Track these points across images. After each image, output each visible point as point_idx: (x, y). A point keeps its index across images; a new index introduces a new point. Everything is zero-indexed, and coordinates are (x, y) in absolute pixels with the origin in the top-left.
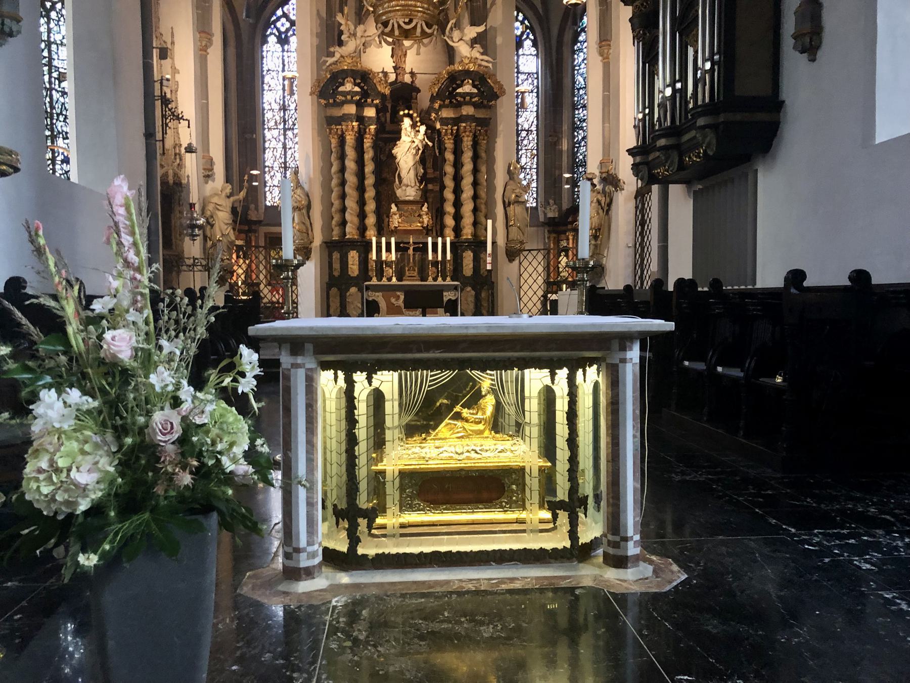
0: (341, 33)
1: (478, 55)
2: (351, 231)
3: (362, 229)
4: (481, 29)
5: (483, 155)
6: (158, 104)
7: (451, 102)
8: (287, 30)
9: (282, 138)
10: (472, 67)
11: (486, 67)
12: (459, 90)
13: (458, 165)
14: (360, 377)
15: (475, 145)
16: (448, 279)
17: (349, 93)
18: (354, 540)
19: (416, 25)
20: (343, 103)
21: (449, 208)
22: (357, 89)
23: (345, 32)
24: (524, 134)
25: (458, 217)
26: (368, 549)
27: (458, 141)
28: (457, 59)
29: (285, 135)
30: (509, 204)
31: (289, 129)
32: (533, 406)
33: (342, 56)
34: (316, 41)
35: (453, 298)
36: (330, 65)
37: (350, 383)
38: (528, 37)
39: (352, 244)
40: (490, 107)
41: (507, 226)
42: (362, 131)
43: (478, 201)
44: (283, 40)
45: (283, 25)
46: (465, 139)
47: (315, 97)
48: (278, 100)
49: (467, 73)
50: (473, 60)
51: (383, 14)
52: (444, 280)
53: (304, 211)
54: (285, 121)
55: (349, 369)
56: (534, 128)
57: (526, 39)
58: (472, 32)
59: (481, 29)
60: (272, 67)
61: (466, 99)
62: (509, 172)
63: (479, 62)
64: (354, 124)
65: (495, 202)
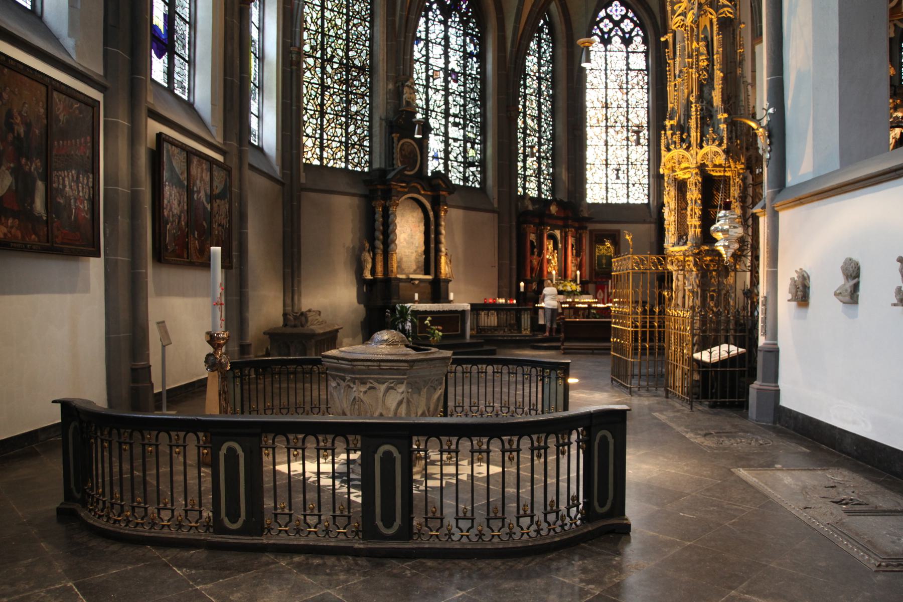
8: (611, 30)
9: (604, 135)
29: (607, 132)
31: (611, 127)
44: (606, 41)
45: (606, 26)
48: (600, 99)
54: (607, 119)
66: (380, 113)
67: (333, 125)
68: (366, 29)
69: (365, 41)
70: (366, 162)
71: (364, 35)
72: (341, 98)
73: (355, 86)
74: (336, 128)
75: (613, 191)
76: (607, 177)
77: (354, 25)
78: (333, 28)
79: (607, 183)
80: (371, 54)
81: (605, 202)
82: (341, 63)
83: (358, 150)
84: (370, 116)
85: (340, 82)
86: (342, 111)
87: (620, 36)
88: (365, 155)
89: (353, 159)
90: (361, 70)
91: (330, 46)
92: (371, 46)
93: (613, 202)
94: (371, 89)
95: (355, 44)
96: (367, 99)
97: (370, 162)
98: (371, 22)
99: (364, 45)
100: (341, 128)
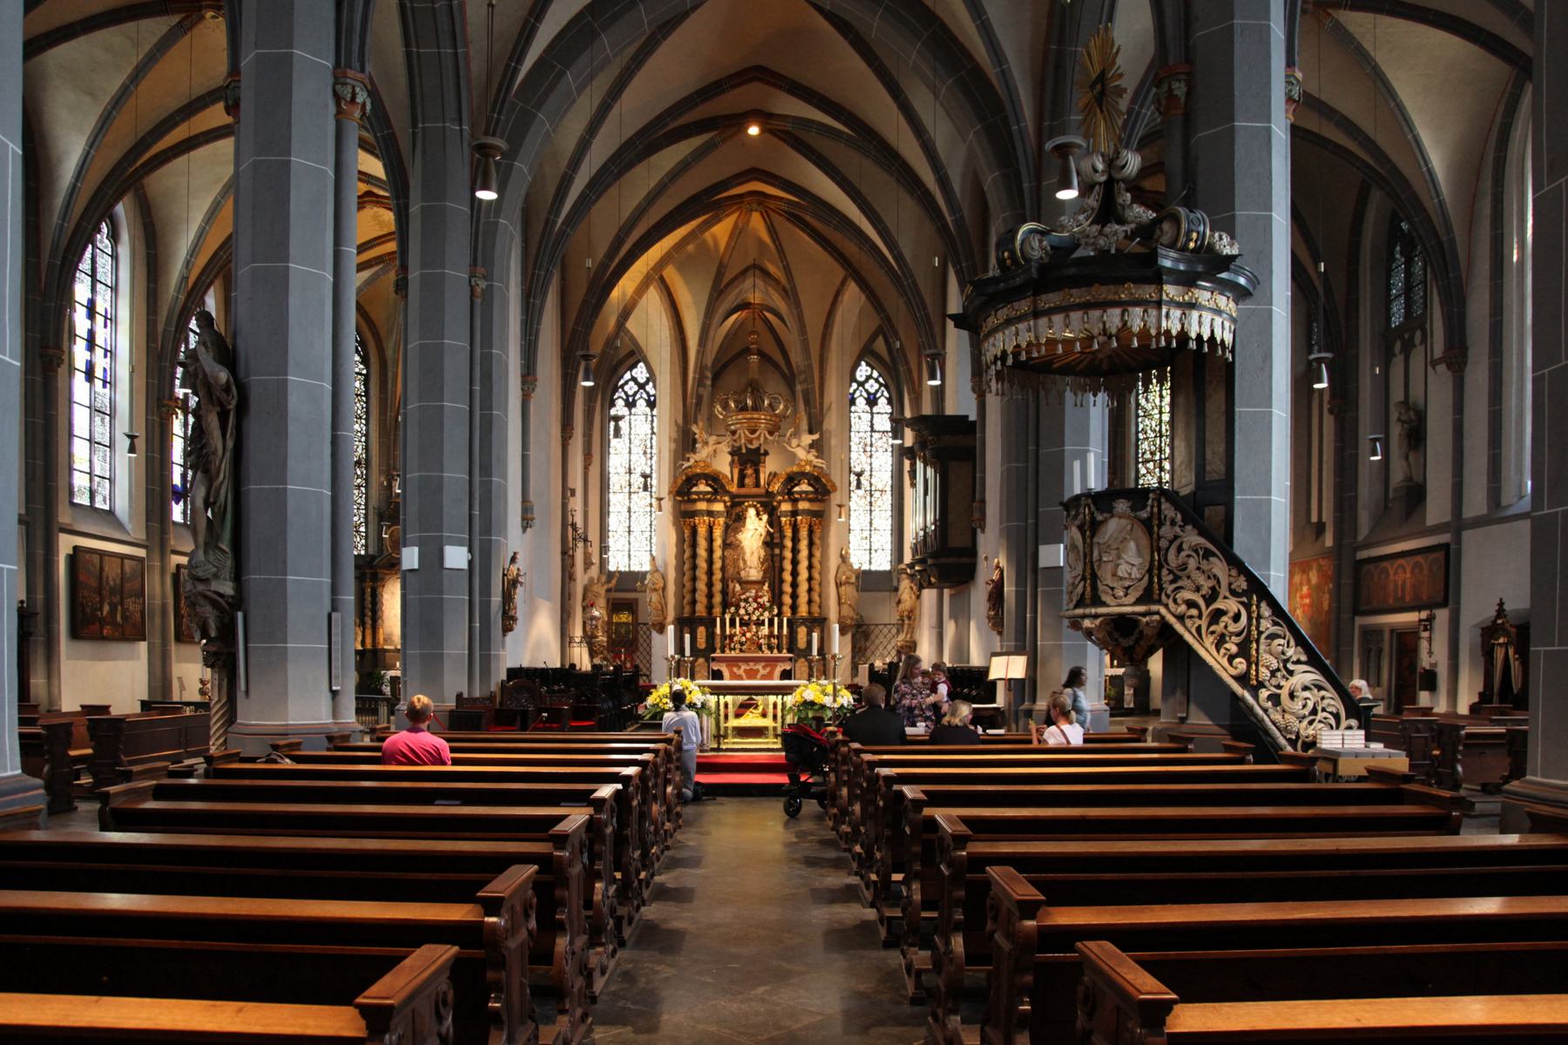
0: (695, 441)
1: (813, 458)
2: (701, 609)
3: (710, 607)
4: (816, 437)
5: (817, 541)
6: (570, 529)
8: (635, 393)
9: (627, 501)
10: (808, 469)
11: (822, 468)
12: (797, 489)
13: (795, 551)
15: (811, 532)
16: (785, 651)
17: (701, 493)
18: (719, 744)
20: (695, 501)
21: (787, 588)
22: (709, 489)
23: (699, 440)
24: (877, 494)
25: (794, 596)
26: (723, 747)
27: (795, 530)
29: (630, 498)
30: (841, 584)
32: (771, 707)
34: (673, 446)
35: (788, 668)
36: (686, 468)
39: (701, 621)
40: (822, 501)
41: (840, 603)
43: (813, 582)
44: (630, 404)
45: (630, 389)
47: (672, 496)
49: (803, 475)
50: (809, 463)
52: (780, 651)
53: (661, 592)
54: (630, 485)
55: (718, 695)
56: (888, 488)
58: (807, 439)
59: (816, 437)
61: (805, 496)
62: (841, 556)
65: (829, 583)
66: (374, 502)
76: (630, 544)
79: (629, 551)
80: (367, 449)
81: (627, 569)
84: (366, 505)
92: (366, 442)
93: (636, 570)
94: (366, 480)
96: (363, 489)
97: (366, 546)
98: (366, 419)
99: (360, 441)
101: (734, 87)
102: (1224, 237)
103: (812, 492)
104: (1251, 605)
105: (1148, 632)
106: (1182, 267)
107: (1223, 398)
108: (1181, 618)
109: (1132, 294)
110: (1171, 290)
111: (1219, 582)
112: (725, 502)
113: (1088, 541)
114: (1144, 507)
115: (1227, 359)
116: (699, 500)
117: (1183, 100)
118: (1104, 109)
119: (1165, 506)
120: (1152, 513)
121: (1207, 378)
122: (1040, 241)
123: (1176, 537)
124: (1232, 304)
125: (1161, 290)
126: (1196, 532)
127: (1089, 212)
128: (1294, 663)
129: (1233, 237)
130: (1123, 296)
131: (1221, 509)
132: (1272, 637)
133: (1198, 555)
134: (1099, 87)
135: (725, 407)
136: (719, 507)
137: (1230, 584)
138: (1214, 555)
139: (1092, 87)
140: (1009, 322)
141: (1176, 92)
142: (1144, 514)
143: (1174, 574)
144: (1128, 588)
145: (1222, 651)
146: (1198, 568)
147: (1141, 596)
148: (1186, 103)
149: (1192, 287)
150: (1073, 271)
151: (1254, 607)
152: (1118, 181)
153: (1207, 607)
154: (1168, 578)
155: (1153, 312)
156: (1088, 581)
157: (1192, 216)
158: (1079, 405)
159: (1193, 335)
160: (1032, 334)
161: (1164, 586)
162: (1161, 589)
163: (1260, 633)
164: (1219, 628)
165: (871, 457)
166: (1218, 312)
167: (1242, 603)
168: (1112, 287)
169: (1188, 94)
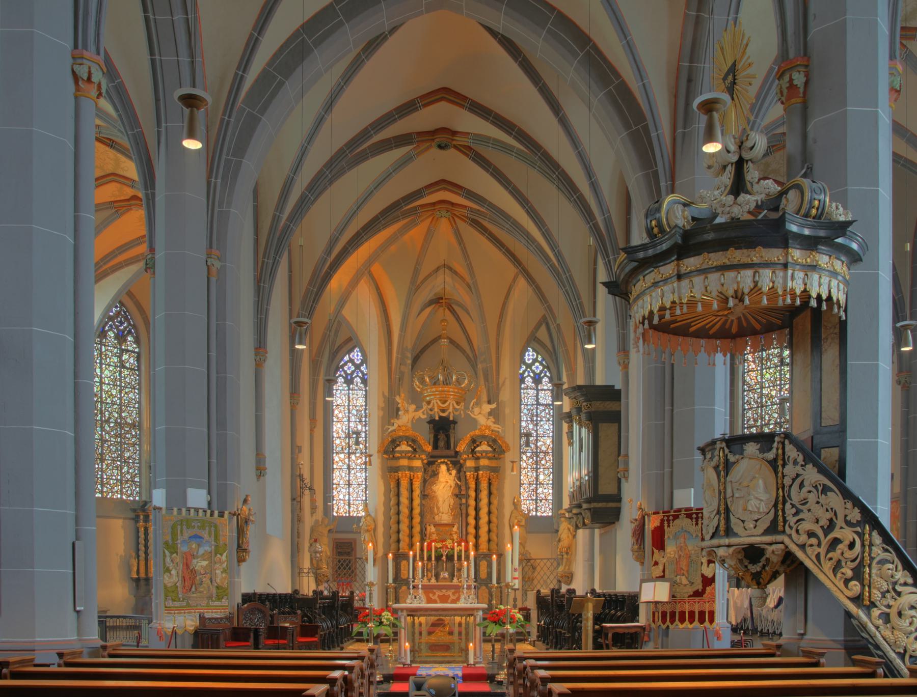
0: (398, 410)
4: (494, 406)
7: (473, 456)
8: (353, 372)
10: (487, 432)
11: (498, 432)
12: (478, 449)
14: (416, 618)
15: (490, 484)
17: (403, 452)
19: (449, 405)
20: (399, 458)
22: (410, 449)
28: (478, 427)
32: (457, 625)
33: (399, 426)
34: (381, 413)
36: (392, 432)
37: (414, 619)
38: (545, 375)
42: (412, 476)
43: (491, 525)
45: (349, 368)
46: (482, 482)
47: (380, 454)
48: (344, 429)
49: (484, 437)
50: (488, 427)
51: (427, 396)
55: (413, 616)
57: (543, 377)
58: (487, 408)
59: (494, 406)
60: (339, 401)
61: (485, 455)
62: (514, 503)
63: (492, 428)
64: (407, 472)
66: (145, 457)
67: (111, 467)
68: (136, 394)
69: (135, 404)
70: (137, 493)
71: (134, 399)
72: (117, 448)
73: (127, 438)
74: (113, 469)
75: (355, 506)
77: (126, 393)
78: (109, 397)
80: (139, 413)
82: (116, 422)
83: (131, 484)
84: (140, 459)
85: (116, 436)
86: (117, 457)
87: (360, 377)
88: (136, 488)
89: (127, 491)
90: (133, 426)
91: (108, 411)
92: (139, 408)
95: (127, 407)
98: (139, 389)
99: (134, 407)
100: (117, 469)
101: (425, 105)
102: (840, 207)
103: (490, 452)
104: (864, 534)
105: (775, 559)
106: (806, 232)
107: (837, 353)
108: (802, 547)
109: (762, 257)
110: (796, 254)
111: (835, 514)
112: (423, 460)
113: (722, 480)
114: (770, 449)
115: (840, 317)
116: (402, 457)
117: (801, 90)
118: (735, 96)
119: (789, 448)
120: (777, 455)
121: (823, 336)
122: (683, 212)
123: (798, 475)
124: (845, 268)
125: (787, 254)
126: (816, 470)
127: (723, 189)
128: (901, 585)
129: (845, 208)
130: (755, 259)
131: (836, 451)
132: (882, 562)
133: (818, 491)
134: (730, 78)
135: (422, 381)
136: (418, 463)
137: (846, 516)
138: (831, 490)
139: (725, 79)
140: (655, 284)
141: (795, 83)
142: (771, 455)
143: (797, 508)
144: (756, 521)
145: (839, 575)
146: (818, 503)
147: (768, 528)
148: (805, 93)
149: (813, 250)
150: (710, 236)
151: (867, 536)
152: (747, 161)
153: (826, 536)
154: (790, 511)
155: (780, 274)
156: (723, 515)
157: (814, 185)
158: (712, 364)
159: (814, 295)
160: (676, 295)
161: (787, 519)
162: (785, 521)
163: (872, 559)
164: (835, 555)
165: (536, 425)
166: (834, 274)
167: (857, 533)
168: (745, 251)
169: (806, 84)
